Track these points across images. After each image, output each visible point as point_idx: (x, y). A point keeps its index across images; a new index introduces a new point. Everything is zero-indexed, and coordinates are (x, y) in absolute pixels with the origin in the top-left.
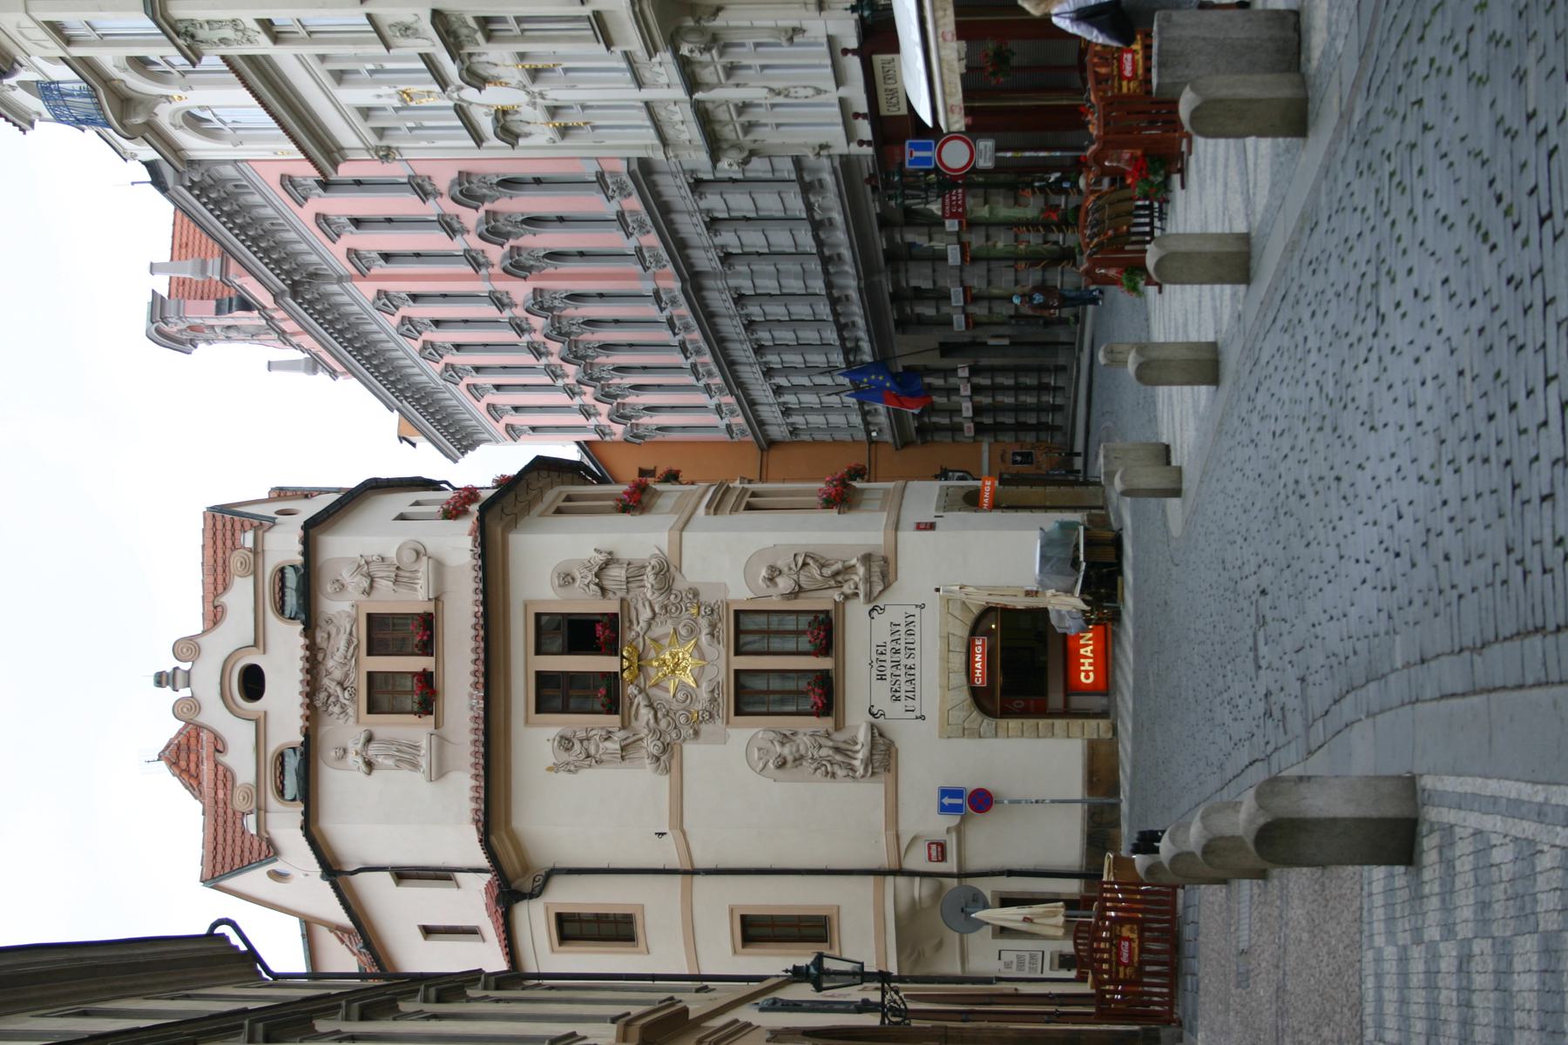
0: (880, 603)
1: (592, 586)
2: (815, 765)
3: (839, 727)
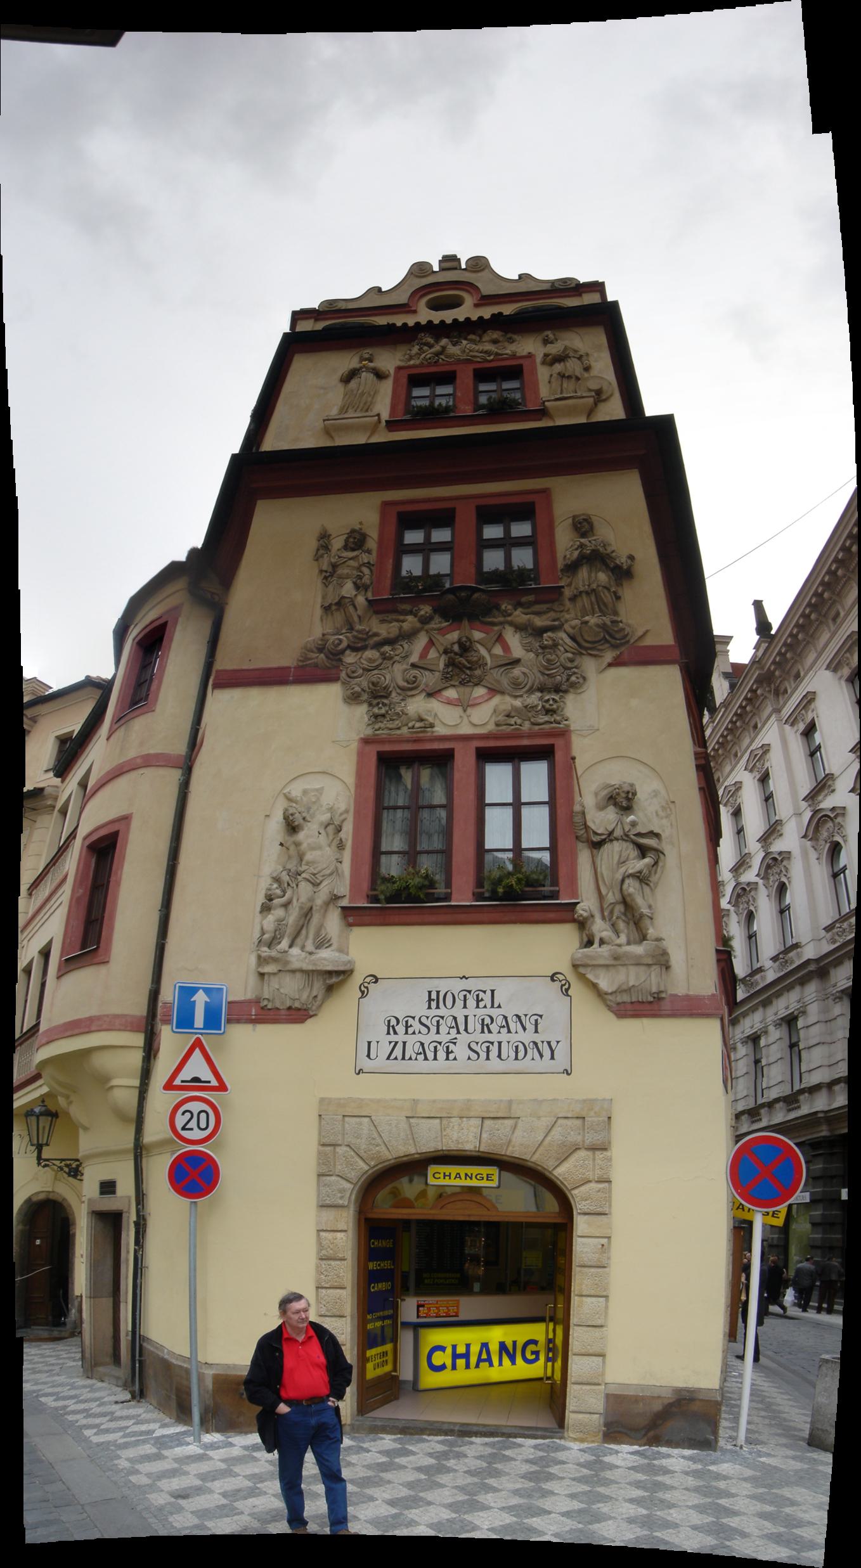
0: (577, 989)
1: (576, 553)
2: (285, 878)
3: (353, 916)
